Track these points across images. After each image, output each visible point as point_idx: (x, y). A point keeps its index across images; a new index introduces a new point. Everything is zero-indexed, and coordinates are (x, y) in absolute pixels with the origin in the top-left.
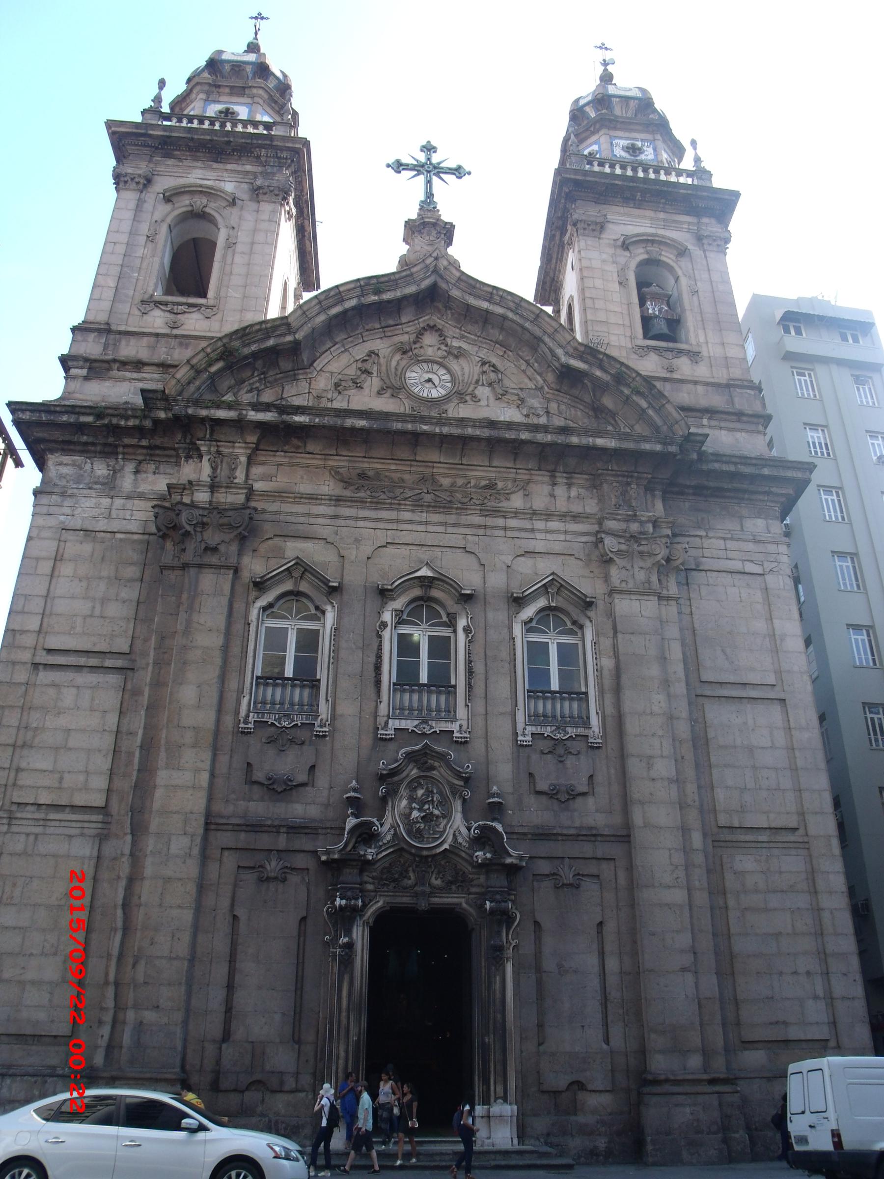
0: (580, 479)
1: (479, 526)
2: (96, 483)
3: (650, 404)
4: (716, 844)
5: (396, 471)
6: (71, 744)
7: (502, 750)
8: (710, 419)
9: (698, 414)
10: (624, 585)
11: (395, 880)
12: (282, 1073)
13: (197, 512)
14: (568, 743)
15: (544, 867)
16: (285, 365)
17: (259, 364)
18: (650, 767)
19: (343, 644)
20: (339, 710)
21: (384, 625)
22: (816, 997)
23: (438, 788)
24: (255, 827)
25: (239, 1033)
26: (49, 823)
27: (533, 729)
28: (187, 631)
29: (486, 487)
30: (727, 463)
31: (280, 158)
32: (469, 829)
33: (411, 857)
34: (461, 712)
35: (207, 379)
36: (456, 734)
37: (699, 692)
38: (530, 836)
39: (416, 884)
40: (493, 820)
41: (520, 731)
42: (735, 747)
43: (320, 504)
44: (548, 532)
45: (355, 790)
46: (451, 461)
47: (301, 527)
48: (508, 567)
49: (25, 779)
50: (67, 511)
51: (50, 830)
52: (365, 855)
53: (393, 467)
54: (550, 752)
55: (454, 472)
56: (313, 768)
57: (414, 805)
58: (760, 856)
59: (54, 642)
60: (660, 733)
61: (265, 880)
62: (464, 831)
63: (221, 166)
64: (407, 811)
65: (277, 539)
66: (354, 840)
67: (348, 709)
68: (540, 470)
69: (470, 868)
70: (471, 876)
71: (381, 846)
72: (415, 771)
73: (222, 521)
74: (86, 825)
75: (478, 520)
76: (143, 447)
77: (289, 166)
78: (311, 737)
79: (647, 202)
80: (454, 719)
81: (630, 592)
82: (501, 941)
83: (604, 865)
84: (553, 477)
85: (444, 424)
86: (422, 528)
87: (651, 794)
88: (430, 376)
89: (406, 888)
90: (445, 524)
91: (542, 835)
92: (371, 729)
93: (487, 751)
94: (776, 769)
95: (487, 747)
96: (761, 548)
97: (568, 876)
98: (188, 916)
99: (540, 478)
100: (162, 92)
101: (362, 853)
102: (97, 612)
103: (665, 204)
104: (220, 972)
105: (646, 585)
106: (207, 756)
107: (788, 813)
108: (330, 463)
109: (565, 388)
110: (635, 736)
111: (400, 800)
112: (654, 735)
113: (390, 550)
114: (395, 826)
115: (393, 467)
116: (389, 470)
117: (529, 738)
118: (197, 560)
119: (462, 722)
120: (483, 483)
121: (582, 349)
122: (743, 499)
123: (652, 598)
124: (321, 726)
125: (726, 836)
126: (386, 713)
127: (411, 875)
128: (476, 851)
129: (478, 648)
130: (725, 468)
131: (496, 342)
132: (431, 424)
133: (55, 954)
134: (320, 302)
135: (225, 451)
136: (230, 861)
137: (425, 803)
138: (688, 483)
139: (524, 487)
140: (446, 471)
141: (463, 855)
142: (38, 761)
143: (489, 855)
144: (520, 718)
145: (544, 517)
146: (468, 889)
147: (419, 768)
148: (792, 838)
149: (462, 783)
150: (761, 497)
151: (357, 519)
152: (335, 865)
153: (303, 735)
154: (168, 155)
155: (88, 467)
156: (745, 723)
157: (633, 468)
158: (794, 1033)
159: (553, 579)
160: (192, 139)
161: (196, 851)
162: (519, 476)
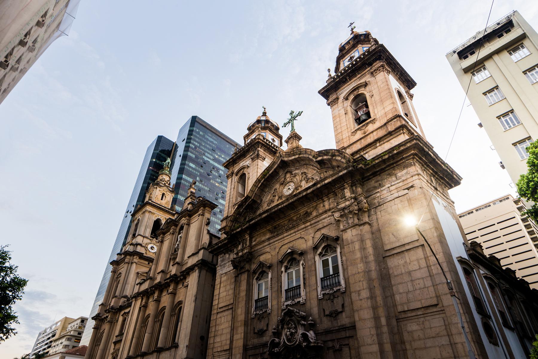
0: (331, 195)
1: (304, 228)
4: (398, 321)
5: (283, 222)
6: (223, 333)
10: (345, 227)
14: (335, 294)
15: (330, 344)
18: (359, 295)
19: (273, 282)
21: (282, 272)
24: (255, 347)
26: (220, 356)
28: (239, 293)
29: (305, 214)
34: (303, 293)
36: (301, 302)
38: (324, 333)
42: (402, 274)
43: (266, 242)
46: (294, 211)
48: (313, 237)
49: (216, 345)
52: (274, 351)
53: (281, 221)
55: (296, 214)
59: (220, 306)
60: (362, 279)
67: (275, 303)
68: (318, 200)
75: (303, 226)
80: (300, 297)
83: (350, 340)
85: (284, 203)
86: (290, 236)
87: (361, 306)
88: (289, 187)
90: (295, 232)
91: (327, 332)
106: (243, 328)
108: (268, 228)
110: (353, 284)
111: (285, 329)
112: (360, 281)
113: (283, 247)
115: (281, 221)
116: (281, 223)
118: (240, 272)
119: (303, 297)
120: (305, 212)
129: (306, 269)
131: (304, 165)
132: (281, 205)
134: (255, 185)
139: (316, 208)
142: (218, 339)
144: (319, 289)
151: (274, 242)
159: (324, 236)
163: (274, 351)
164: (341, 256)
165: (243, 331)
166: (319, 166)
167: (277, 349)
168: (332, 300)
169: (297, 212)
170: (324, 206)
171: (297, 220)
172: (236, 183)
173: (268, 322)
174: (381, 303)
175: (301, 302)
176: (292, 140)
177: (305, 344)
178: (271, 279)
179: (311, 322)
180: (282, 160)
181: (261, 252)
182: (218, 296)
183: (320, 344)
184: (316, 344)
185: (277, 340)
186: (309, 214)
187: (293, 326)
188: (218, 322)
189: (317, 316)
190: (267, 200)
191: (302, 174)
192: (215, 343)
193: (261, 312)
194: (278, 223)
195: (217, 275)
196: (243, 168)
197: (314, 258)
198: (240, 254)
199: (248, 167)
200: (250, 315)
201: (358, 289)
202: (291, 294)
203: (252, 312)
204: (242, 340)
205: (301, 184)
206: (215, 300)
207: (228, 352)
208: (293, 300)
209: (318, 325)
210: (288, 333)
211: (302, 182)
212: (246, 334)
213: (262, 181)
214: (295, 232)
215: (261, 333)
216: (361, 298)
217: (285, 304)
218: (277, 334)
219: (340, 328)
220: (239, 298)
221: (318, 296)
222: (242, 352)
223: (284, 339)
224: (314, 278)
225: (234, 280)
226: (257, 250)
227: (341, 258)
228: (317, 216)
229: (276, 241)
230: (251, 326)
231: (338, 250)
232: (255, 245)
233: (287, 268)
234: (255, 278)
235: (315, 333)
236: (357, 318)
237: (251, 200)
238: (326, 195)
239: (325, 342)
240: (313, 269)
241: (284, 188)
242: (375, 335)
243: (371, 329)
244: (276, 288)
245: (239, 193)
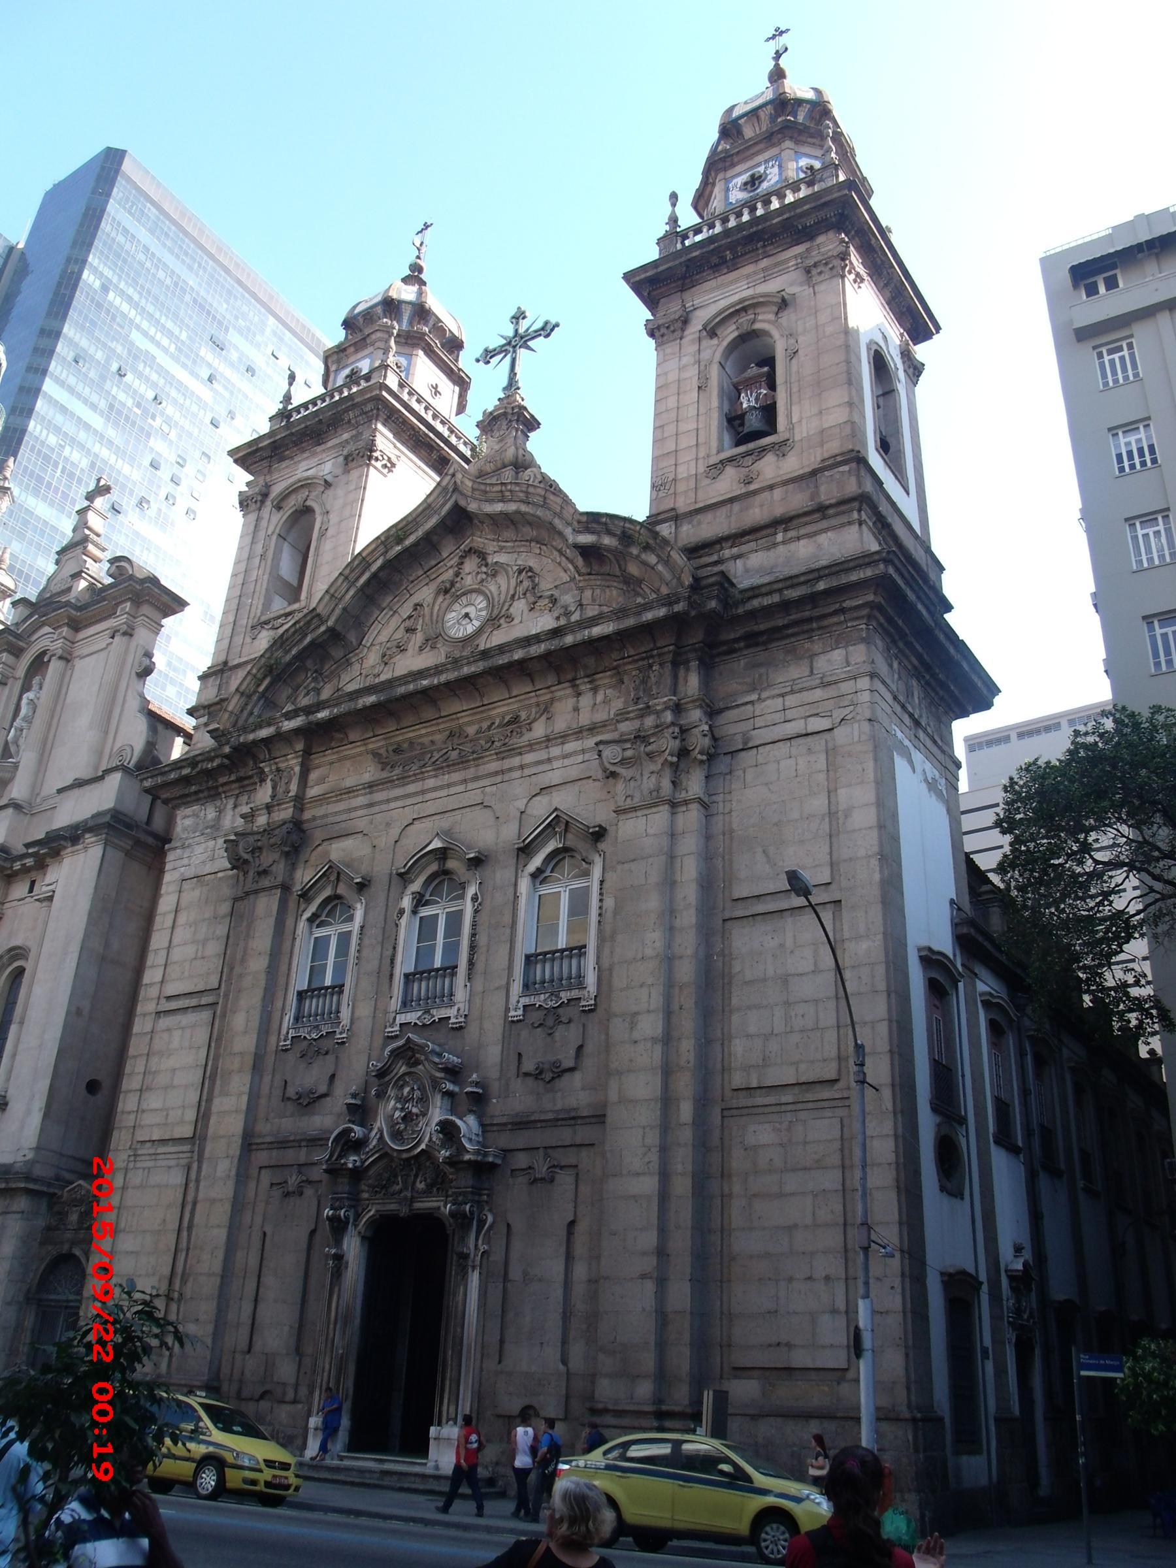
0: (604, 679)
1: (496, 773)
2: (207, 828)
3: (658, 556)
6: (176, 1082)
7: (493, 1029)
8: (786, 530)
9: (769, 531)
11: (384, 1187)
12: (284, 1384)
13: (251, 839)
14: (560, 1011)
15: (522, 1160)
16: (337, 653)
17: (309, 663)
18: (633, 1025)
19: (366, 941)
20: (357, 1014)
21: (402, 912)
22: (834, 1311)
24: (282, 1144)
25: (258, 1346)
28: (243, 960)
29: (509, 723)
30: (770, 593)
31: (366, 413)
34: (461, 995)
35: (259, 699)
36: (453, 1020)
37: (727, 915)
38: (510, 1127)
43: (357, 796)
44: (565, 757)
47: (343, 825)
49: (148, 1119)
50: (185, 861)
51: (159, 1163)
52: (345, 1164)
53: (423, 731)
54: (541, 1025)
55: (478, 717)
56: (333, 1076)
58: (780, 1123)
59: (171, 990)
60: (650, 981)
61: (287, 1195)
63: (323, 447)
65: (325, 843)
66: (339, 1149)
67: (364, 1010)
68: (559, 683)
72: (403, 1068)
73: (272, 841)
74: (181, 1155)
75: (494, 766)
76: (233, 782)
77: (378, 416)
79: (742, 255)
80: (451, 1005)
81: (634, 809)
82: (469, 1248)
83: (584, 1153)
84: (574, 686)
85: (441, 672)
86: (444, 793)
87: (631, 1061)
90: (465, 781)
91: (522, 1124)
94: (816, 1001)
96: (831, 692)
97: (542, 1170)
98: (222, 1234)
99: (562, 693)
100: (292, 388)
102: (200, 954)
103: (764, 246)
104: (251, 1286)
105: (654, 794)
106: (247, 1078)
107: (825, 1060)
109: (596, 567)
110: (622, 990)
113: (418, 825)
114: (381, 1131)
115: (423, 731)
116: (421, 736)
118: (255, 887)
119: (461, 1006)
120: (507, 718)
121: (584, 519)
122: (813, 630)
123: (661, 808)
125: (743, 1100)
129: (484, 917)
130: (767, 601)
131: (530, 541)
133: (154, 1274)
134: (346, 578)
135: (282, 765)
136: (266, 1178)
138: (732, 636)
139: (546, 710)
140: (470, 718)
142: (153, 1101)
144: (517, 988)
145: (560, 740)
148: (827, 1094)
150: (835, 619)
151: (388, 801)
153: (327, 1044)
154: (282, 459)
155: (202, 814)
156: (782, 945)
157: (652, 646)
158: (800, 1359)
160: (292, 434)
161: (233, 1172)
162: (542, 699)
164: (601, 894)
165: (246, 1089)
166: (580, 561)
167: (356, 1158)
168: (551, 1028)
169: (482, 712)
170: (576, 709)
171: (478, 739)
172: (274, 537)
173: (336, 1069)
174: (692, 1058)
175: (453, 1020)
176: (504, 427)
177: (448, 1154)
178: (362, 927)
179: (475, 1090)
180: (456, 506)
181: (337, 827)
182: (164, 953)
183: (491, 1159)
184: (479, 1158)
185: (358, 1132)
186: (520, 727)
187: (417, 1094)
188: (158, 1044)
189: (494, 1073)
190: (383, 638)
191: (520, 572)
192: (143, 1111)
193: (314, 1036)
194: (411, 735)
195: (168, 877)
196: (306, 485)
197: (516, 885)
198: (262, 820)
199: (328, 484)
200: (273, 1039)
201: (634, 1009)
202: (420, 988)
203: (284, 1031)
204: (242, 1117)
205: (512, 610)
206: (152, 967)
207: (186, 1148)
208: (427, 1012)
210: (397, 1114)
211: (515, 603)
212: (254, 1096)
213: (374, 568)
214: (465, 781)
215: (308, 1101)
216: (636, 1035)
217: (398, 1022)
218: (360, 1111)
219: (561, 1116)
220: (241, 976)
221: (507, 1010)
222: (238, 1152)
223: (381, 1131)
224: (504, 950)
225: (230, 909)
226: (325, 816)
227: (601, 900)
228: (548, 740)
229: (396, 799)
230: (273, 1076)
231: (597, 872)
232: (322, 799)
233: (420, 901)
234: (307, 915)
235: (482, 1125)
236: (613, 1096)
237: (323, 628)
238: (589, 672)
239: (506, 1152)
240: (507, 919)
241: (448, 608)
242: (655, 1150)
243: (647, 1130)
244: (376, 963)
245: (280, 578)
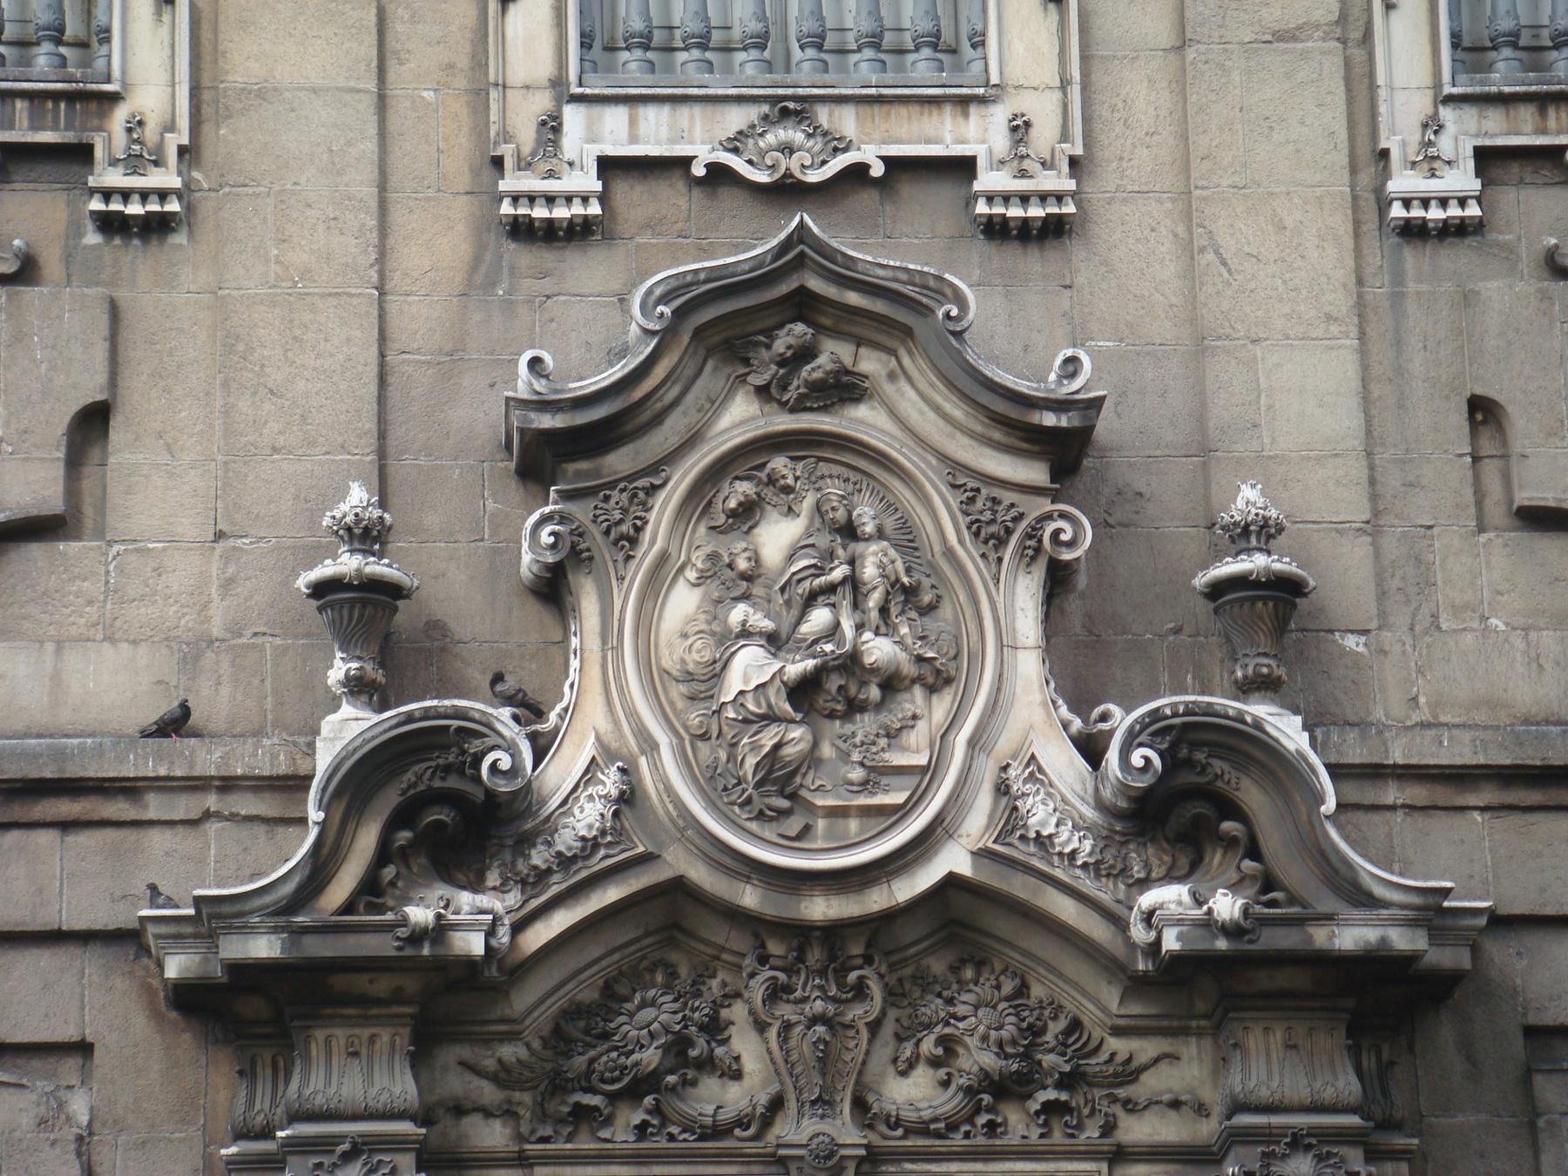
11: (640, 1086)
23: (890, 506)
27: (1500, 130)
32: (1091, 749)
33: (738, 941)
36: (989, 179)
39: (776, 1104)
40: (1250, 687)
41: (1400, 134)
45: (366, 536)
57: (738, 614)
62: (1064, 763)
64: (700, 653)
66: (366, 840)
69: (1111, 996)
70: (1119, 1046)
71: (543, 875)
78: (76, 231)
89: (718, 1131)
92: (458, 163)
93: (1190, 273)
95: (1188, 250)
101: (420, 914)
117: (1463, 179)
124: (134, 163)
126: (544, 69)
127: (746, 1046)
128: (1144, 884)
137: (811, 600)
141: (1065, 909)
143: (1226, 906)
146: (1109, 1129)
147: (763, 392)
149: (1036, 473)
152: (253, 1007)
163: (441, 930)
209: (1351, 642)
